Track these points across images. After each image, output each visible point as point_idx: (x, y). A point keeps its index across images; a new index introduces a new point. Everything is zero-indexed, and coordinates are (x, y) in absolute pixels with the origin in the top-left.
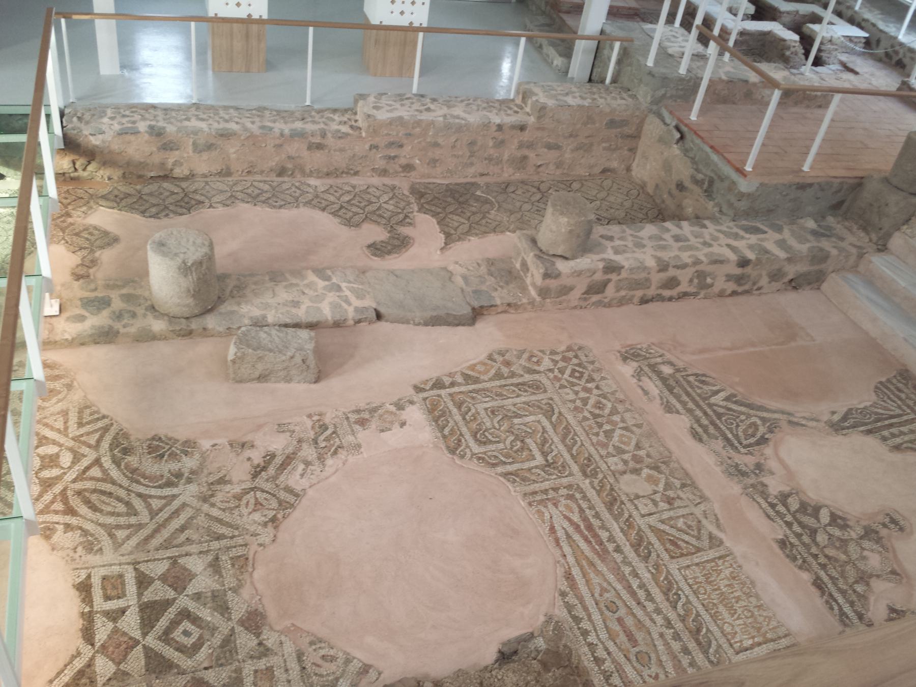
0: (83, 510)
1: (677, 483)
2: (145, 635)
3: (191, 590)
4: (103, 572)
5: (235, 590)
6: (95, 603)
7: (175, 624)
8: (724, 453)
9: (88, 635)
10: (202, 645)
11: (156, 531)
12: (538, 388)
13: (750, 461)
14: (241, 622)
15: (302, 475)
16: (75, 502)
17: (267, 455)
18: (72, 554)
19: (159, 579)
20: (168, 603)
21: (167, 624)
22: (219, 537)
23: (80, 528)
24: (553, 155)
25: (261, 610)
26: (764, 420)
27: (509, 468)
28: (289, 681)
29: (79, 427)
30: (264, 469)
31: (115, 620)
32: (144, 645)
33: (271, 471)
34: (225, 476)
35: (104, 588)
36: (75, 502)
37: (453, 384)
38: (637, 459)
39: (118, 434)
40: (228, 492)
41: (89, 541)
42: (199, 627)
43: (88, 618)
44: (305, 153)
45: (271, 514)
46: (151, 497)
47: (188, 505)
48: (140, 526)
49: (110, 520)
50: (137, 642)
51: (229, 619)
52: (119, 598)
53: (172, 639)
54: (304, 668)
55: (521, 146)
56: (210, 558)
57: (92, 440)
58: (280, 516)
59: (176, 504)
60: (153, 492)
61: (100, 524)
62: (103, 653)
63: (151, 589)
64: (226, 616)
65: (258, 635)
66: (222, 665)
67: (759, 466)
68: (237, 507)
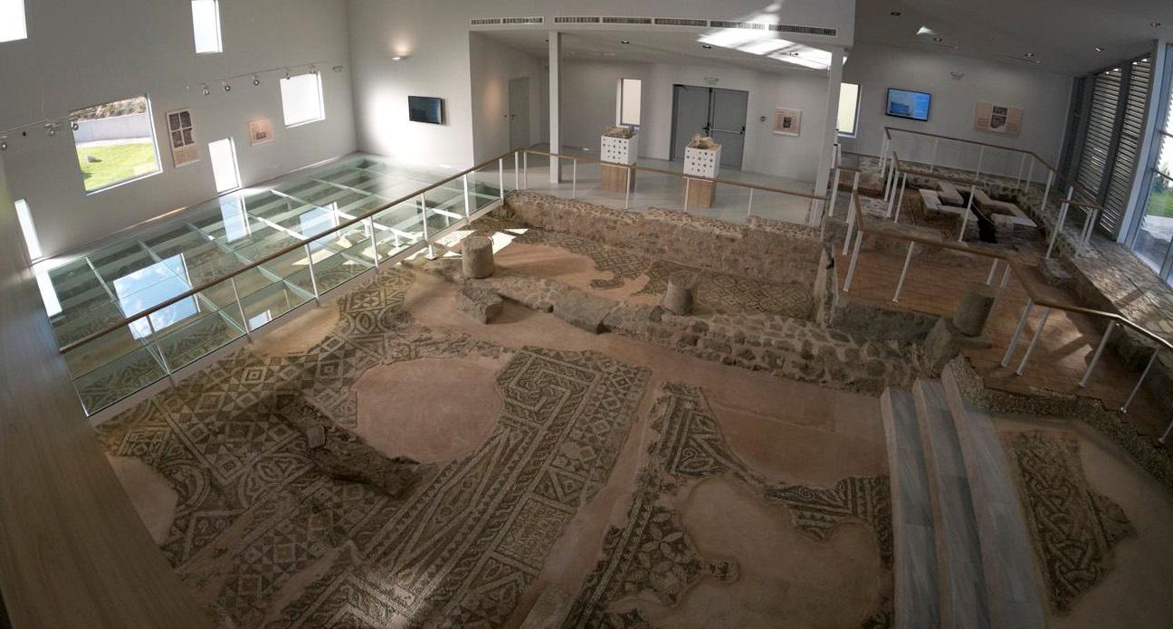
1: (599, 463)
8: (657, 466)
12: (589, 377)
13: (669, 479)
24: (755, 263)
26: (717, 462)
27: (515, 402)
37: (545, 354)
38: (593, 440)
44: (605, 229)
55: (733, 252)
67: (669, 487)
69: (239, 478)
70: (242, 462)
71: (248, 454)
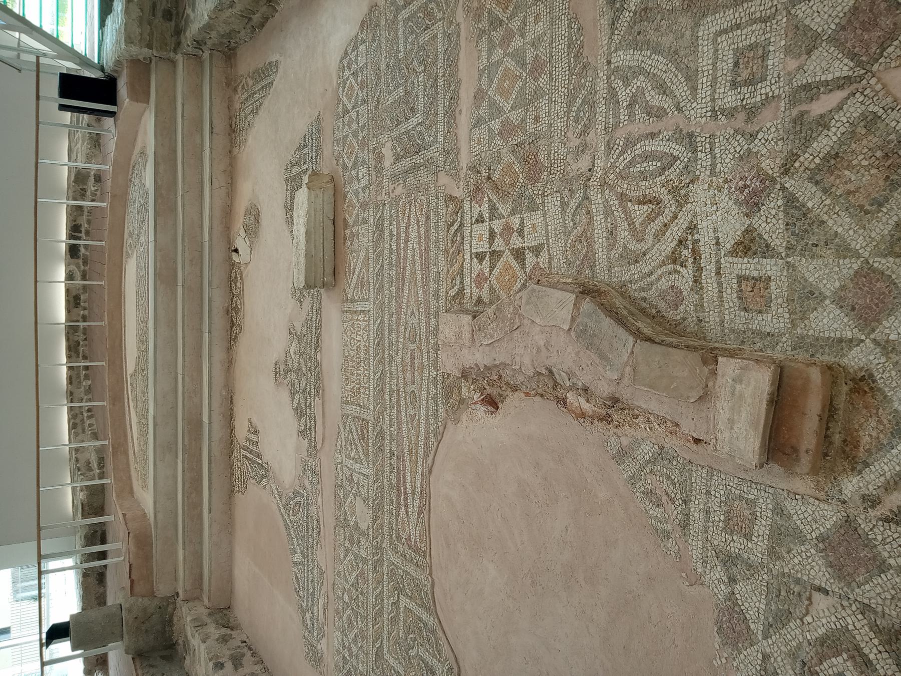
28: (708, 493)
54: (685, 502)
66: (798, 581)
69: (691, 78)
70: (730, 113)
71: (740, 145)
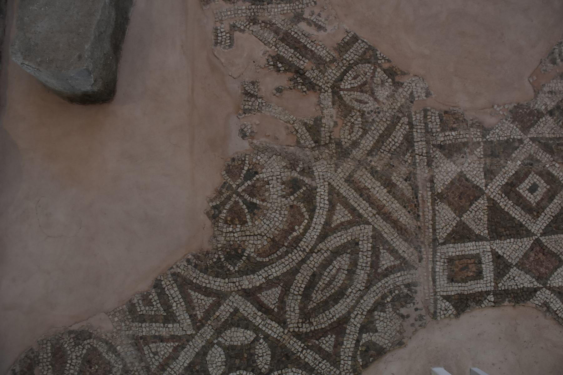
0: (339, 310)
2: (529, 234)
3: (480, 181)
4: (442, 281)
5: (485, 131)
6: (484, 289)
7: (520, 201)
9: (521, 296)
10: (549, 174)
11: (387, 217)
14: (525, 129)
15: (320, 28)
16: (323, 321)
17: (275, 65)
18: (411, 320)
19: (461, 216)
20: (493, 207)
21: (519, 209)
22: (409, 140)
23: (371, 312)
25: (511, 107)
29: (175, 321)
30: (300, 73)
31: (508, 266)
32: (542, 235)
33: (305, 64)
34: (305, 124)
35: (465, 280)
36: (323, 321)
39: (196, 266)
40: (336, 124)
41: (393, 300)
42: (526, 176)
43: (502, 296)
45: (380, 75)
46: (328, 223)
47: (350, 176)
48: (377, 237)
49: (362, 276)
50: (537, 241)
51: (521, 141)
52: (480, 263)
53: (538, 204)
56: (438, 154)
57: (203, 302)
58: (386, 66)
59: (345, 190)
60: (320, 220)
61: (367, 288)
62: (547, 279)
63: (472, 226)
64: (517, 144)
65: (540, 115)
68: (363, 115)
